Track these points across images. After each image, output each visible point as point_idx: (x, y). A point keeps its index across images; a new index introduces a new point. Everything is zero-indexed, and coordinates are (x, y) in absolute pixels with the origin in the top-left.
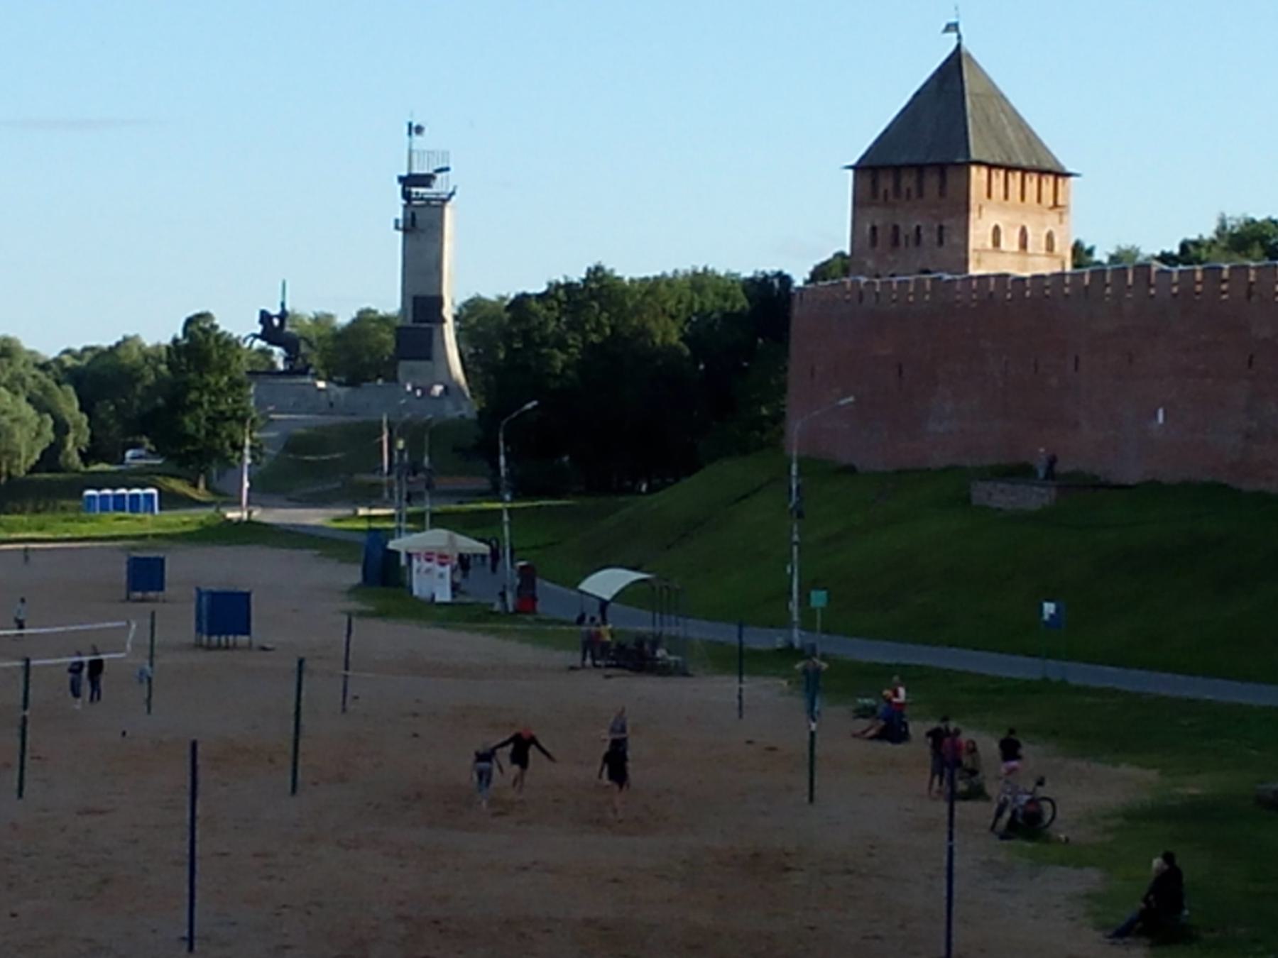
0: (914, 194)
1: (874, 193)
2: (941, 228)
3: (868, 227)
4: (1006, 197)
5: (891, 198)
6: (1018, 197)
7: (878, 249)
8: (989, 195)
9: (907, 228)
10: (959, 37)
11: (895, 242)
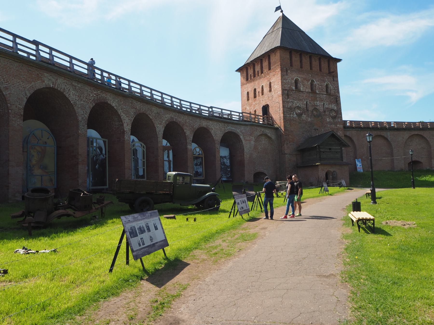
1: (247, 79)
2: (270, 83)
5: (252, 78)
7: (250, 101)
8: (291, 65)
9: (259, 90)
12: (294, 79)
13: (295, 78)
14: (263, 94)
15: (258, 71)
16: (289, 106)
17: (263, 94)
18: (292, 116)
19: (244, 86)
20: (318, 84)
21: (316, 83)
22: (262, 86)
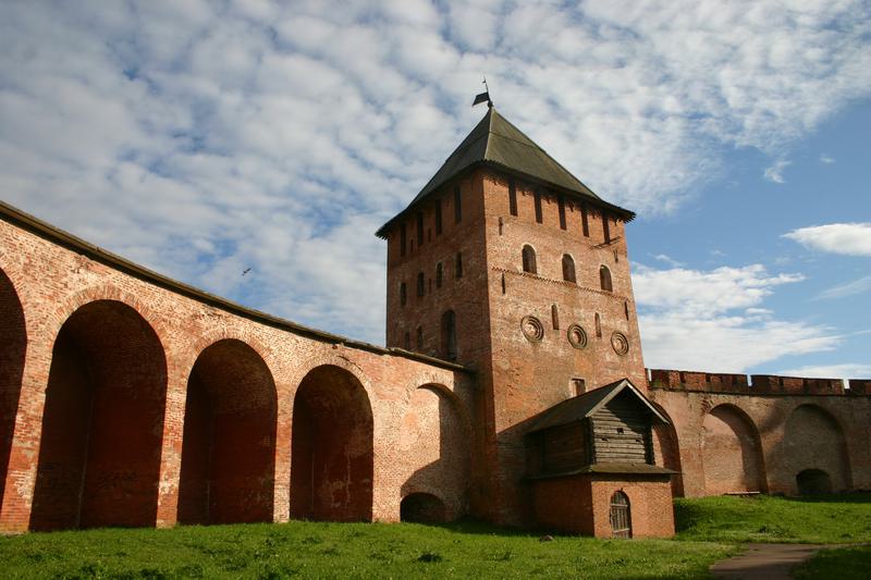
2: (459, 256)
5: (416, 246)
8: (514, 211)
10: (490, 105)
13: (523, 244)
14: (439, 286)
15: (430, 231)
16: (507, 314)
17: (439, 286)
18: (514, 338)
20: (581, 266)
22: (440, 265)
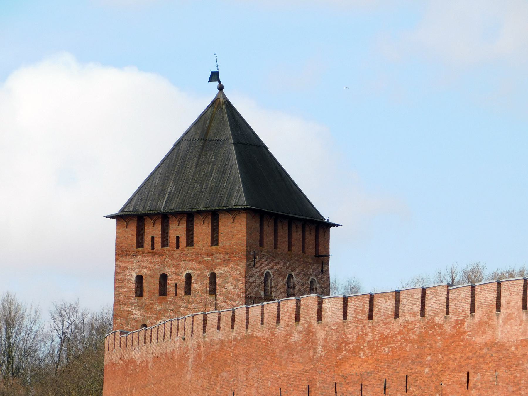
0: (183, 242)
1: (140, 243)
2: (213, 276)
3: (134, 275)
4: (276, 247)
6: (286, 246)
7: (146, 298)
8: (261, 244)
10: (221, 88)
11: (163, 292)
12: (264, 275)
14: (188, 291)
15: (178, 238)
19: (128, 258)
21: (295, 279)
